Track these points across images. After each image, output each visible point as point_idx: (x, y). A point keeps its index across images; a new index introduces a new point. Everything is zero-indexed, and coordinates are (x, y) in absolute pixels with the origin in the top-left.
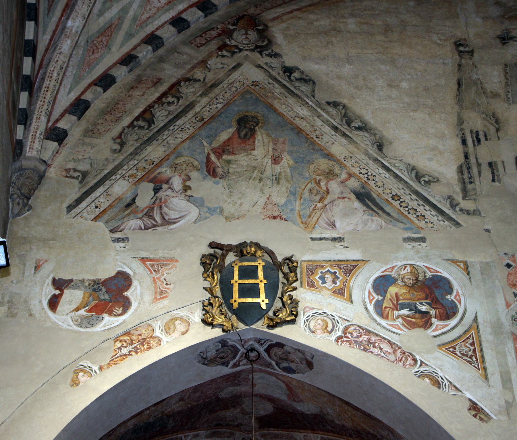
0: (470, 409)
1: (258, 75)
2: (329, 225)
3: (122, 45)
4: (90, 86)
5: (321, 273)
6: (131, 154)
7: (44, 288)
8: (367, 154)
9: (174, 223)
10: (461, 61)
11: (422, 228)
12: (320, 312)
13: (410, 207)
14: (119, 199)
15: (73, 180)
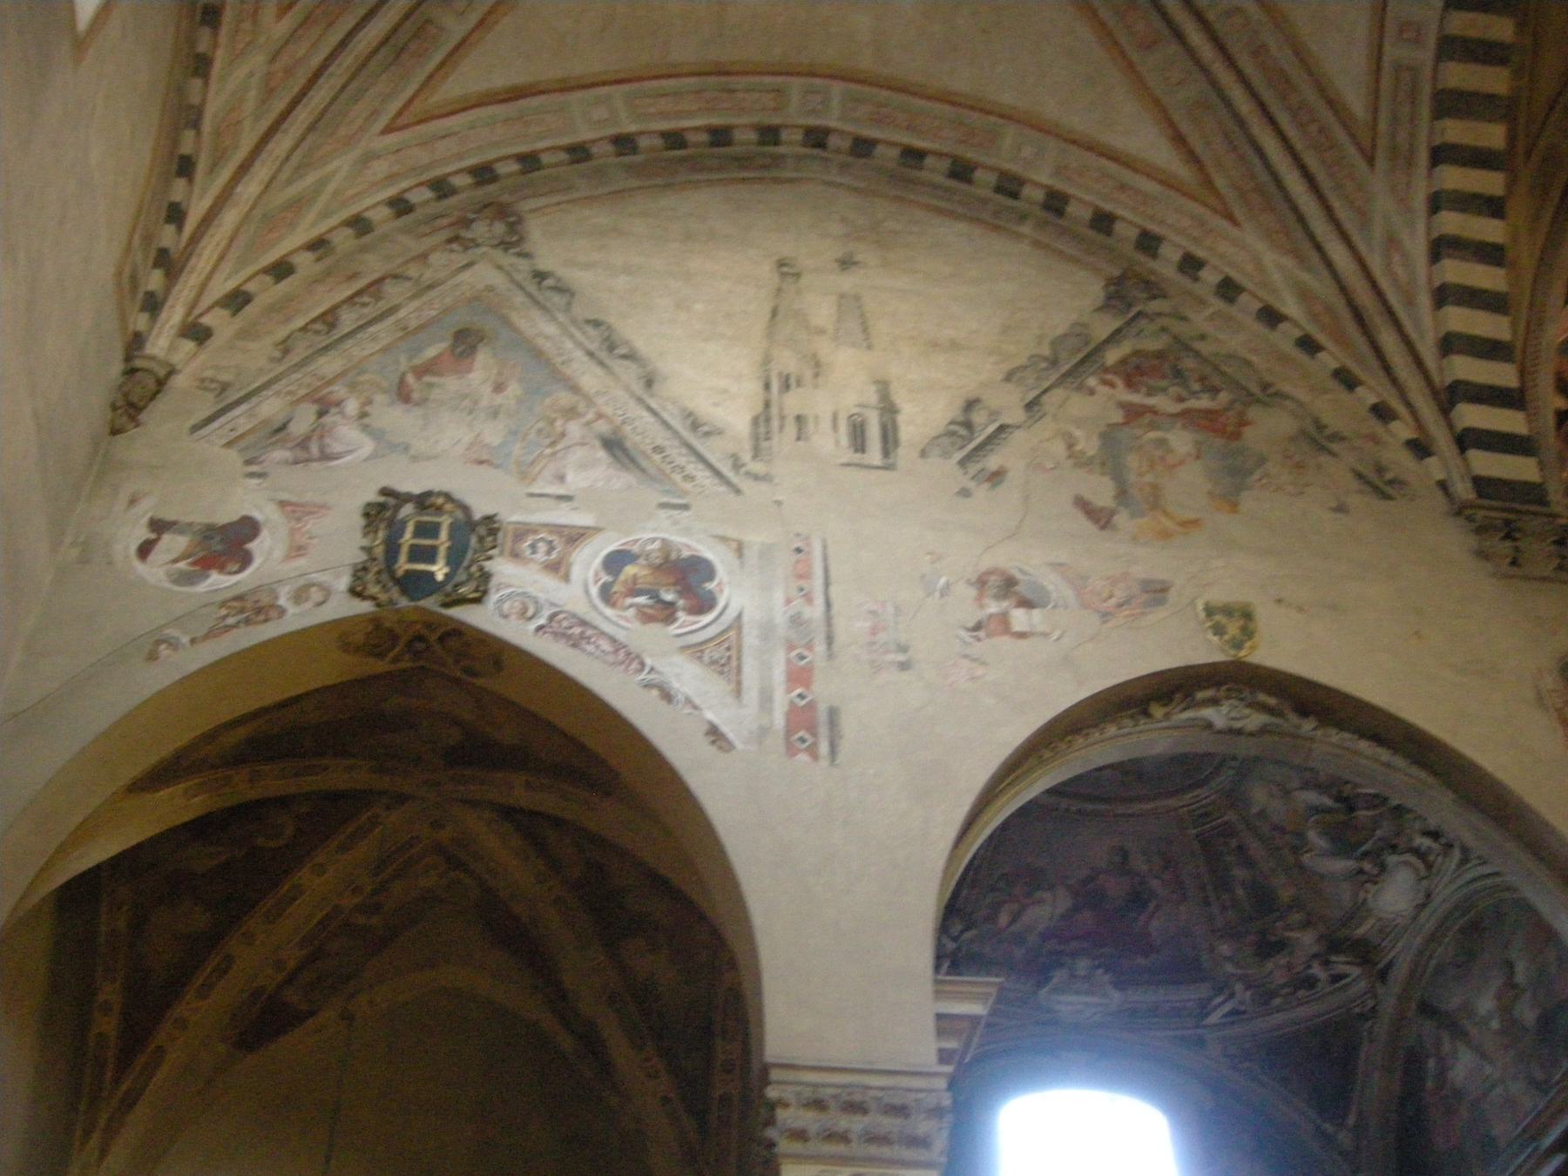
1: (497, 279)
3: (313, 225)
4: (257, 273)
6: (296, 365)
8: (627, 388)
9: (337, 458)
14: (265, 422)
15: (207, 394)
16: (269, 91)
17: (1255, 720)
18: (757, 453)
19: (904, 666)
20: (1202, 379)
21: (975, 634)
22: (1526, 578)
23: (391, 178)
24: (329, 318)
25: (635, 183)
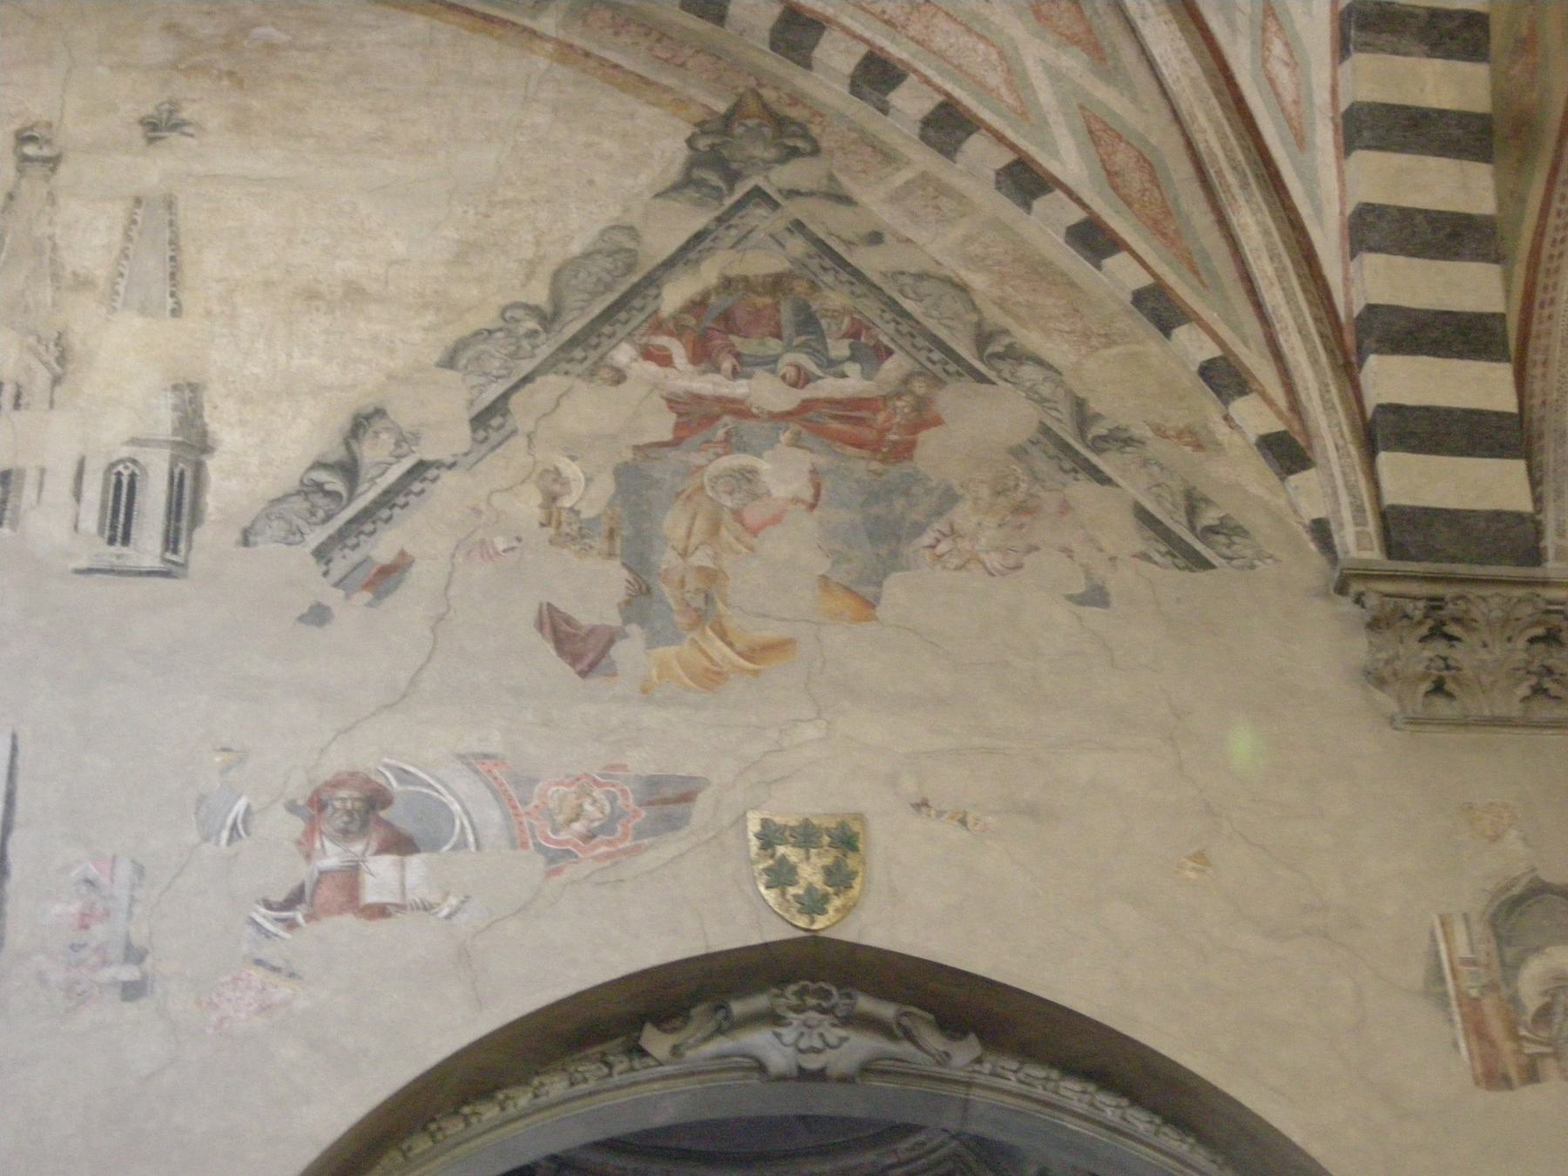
10: (17, 185)
17: (859, 1046)
19: (132, 991)
20: (854, 335)
21: (285, 914)
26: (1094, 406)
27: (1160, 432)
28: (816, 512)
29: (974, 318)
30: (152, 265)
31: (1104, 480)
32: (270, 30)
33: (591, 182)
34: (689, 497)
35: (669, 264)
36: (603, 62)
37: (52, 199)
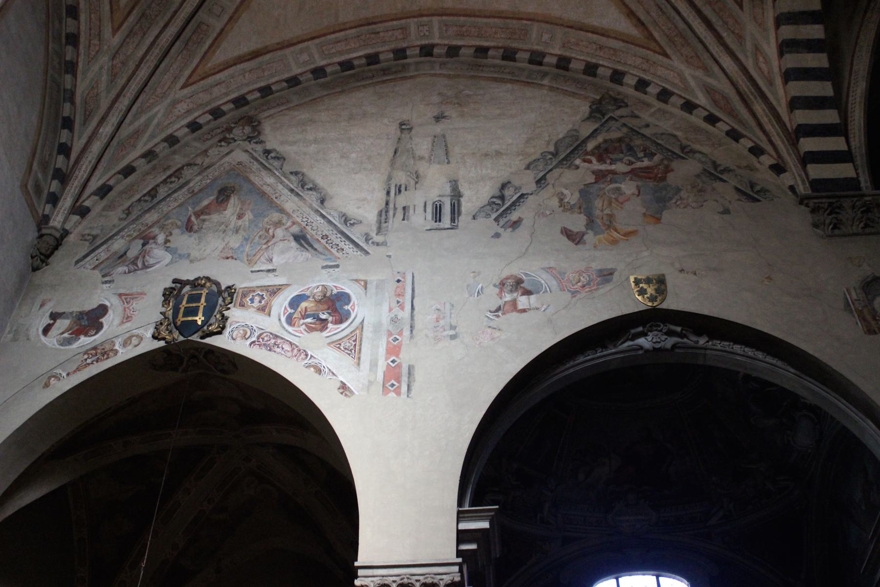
0: (339, 389)
2: (267, 260)
3: (145, 144)
5: (253, 296)
6: (133, 220)
7: (43, 320)
8: (311, 207)
9: (151, 267)
11: (339, 258)
12: (243, 324)
13: (334, 243)
14: (116, 253)
15: (85, 242)
16: (113, 76)
17: (670, 342)
18: (379, 230)
19: (453, 337)
20: (644, 150)
22: (844, 235)
23: (189, 112)
24: (152, 193)
25: (325, 93)
26: (718, 162)
27: (739, 167)
28: (640, 197)
29: (679, 143)
30: (441, 152)
31: (725, 181)
32: (467, 91)
33: (563, 120)
34: (602, 196)
35: (589, 137)
36: (562, 90)
37: (411, 138)
